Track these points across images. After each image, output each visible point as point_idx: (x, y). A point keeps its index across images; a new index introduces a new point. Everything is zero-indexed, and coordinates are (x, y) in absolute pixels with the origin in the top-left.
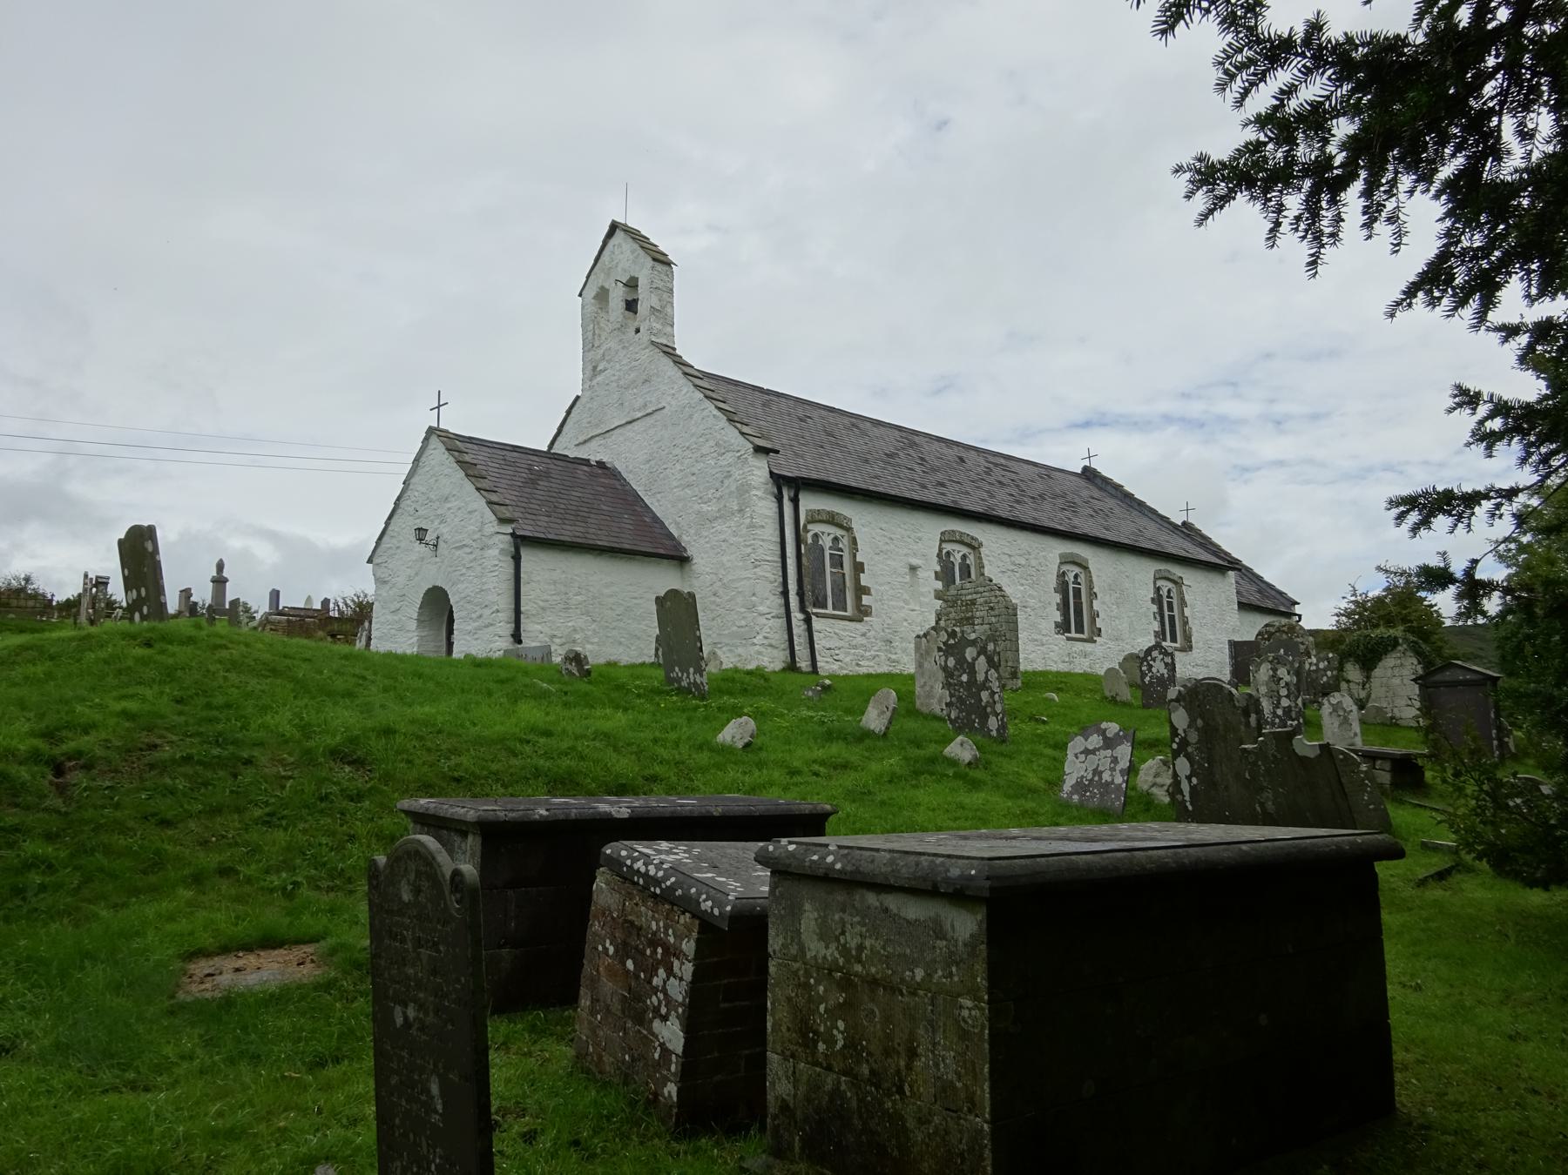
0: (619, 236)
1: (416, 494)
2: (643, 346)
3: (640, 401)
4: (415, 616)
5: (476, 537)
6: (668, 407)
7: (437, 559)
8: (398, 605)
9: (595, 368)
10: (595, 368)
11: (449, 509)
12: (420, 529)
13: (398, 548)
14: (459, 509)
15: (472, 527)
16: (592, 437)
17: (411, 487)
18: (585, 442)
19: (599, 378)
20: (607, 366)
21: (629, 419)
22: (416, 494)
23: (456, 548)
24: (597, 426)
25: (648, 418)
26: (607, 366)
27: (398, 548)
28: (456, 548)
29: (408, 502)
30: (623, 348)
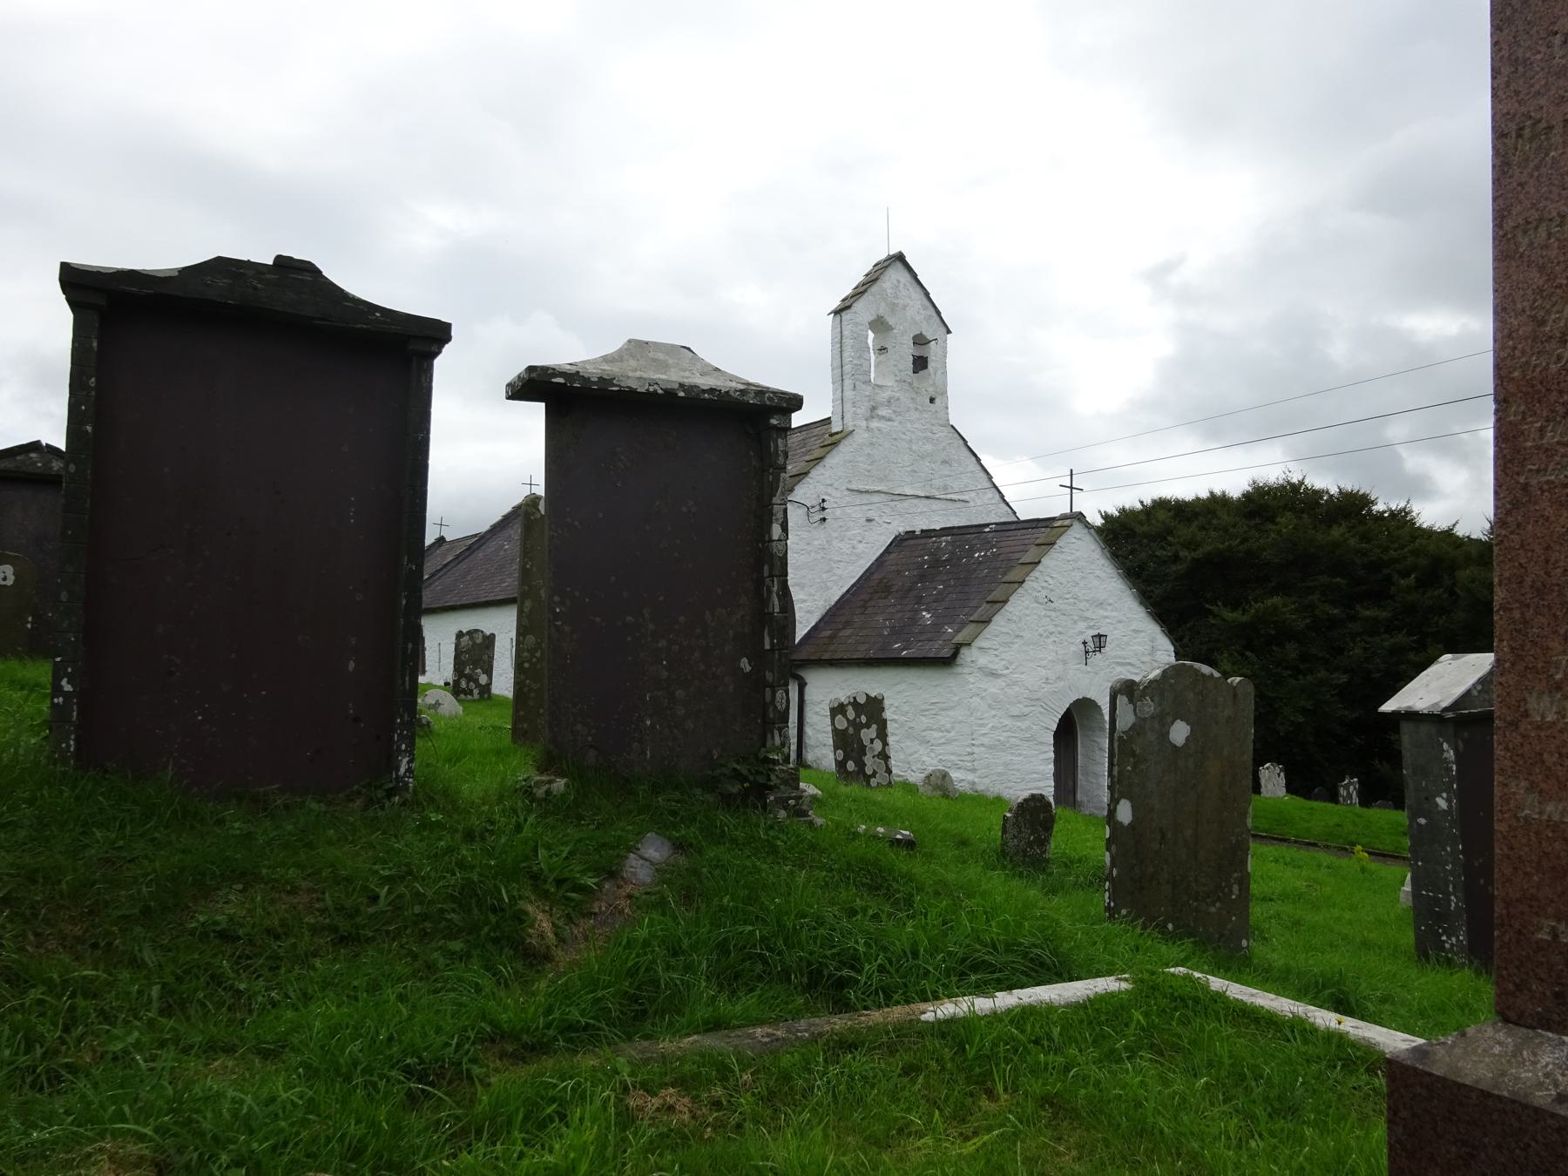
0: (896, 275)
1: (1048, 579)
2: (941, 422)
3: (937, 482)
4: (1054, 727)
5: (1144, 659)
6: (972, 504)
7: (1089, 668)
8: (1026, 710)
9: (874, 408)
10: (874, 408)
11: (1106, 617)
12: (1100, 636)
13: (1017, 636)
14: (1120, 622)
15: (1140, 648)
16: (879, 492)
17: (1040, 567)
18: (867, 492)
19: (875, 424)
20: (893, 416)
21: (928, 494)
22: (1048, 579)
23: (1118, 664)
24: (881, 480)
25: (950, 503)
26: (893, 416)
27: (1017, 636)
28: (1118, 664)
29: (1035, 585)
30: (917, 409)
